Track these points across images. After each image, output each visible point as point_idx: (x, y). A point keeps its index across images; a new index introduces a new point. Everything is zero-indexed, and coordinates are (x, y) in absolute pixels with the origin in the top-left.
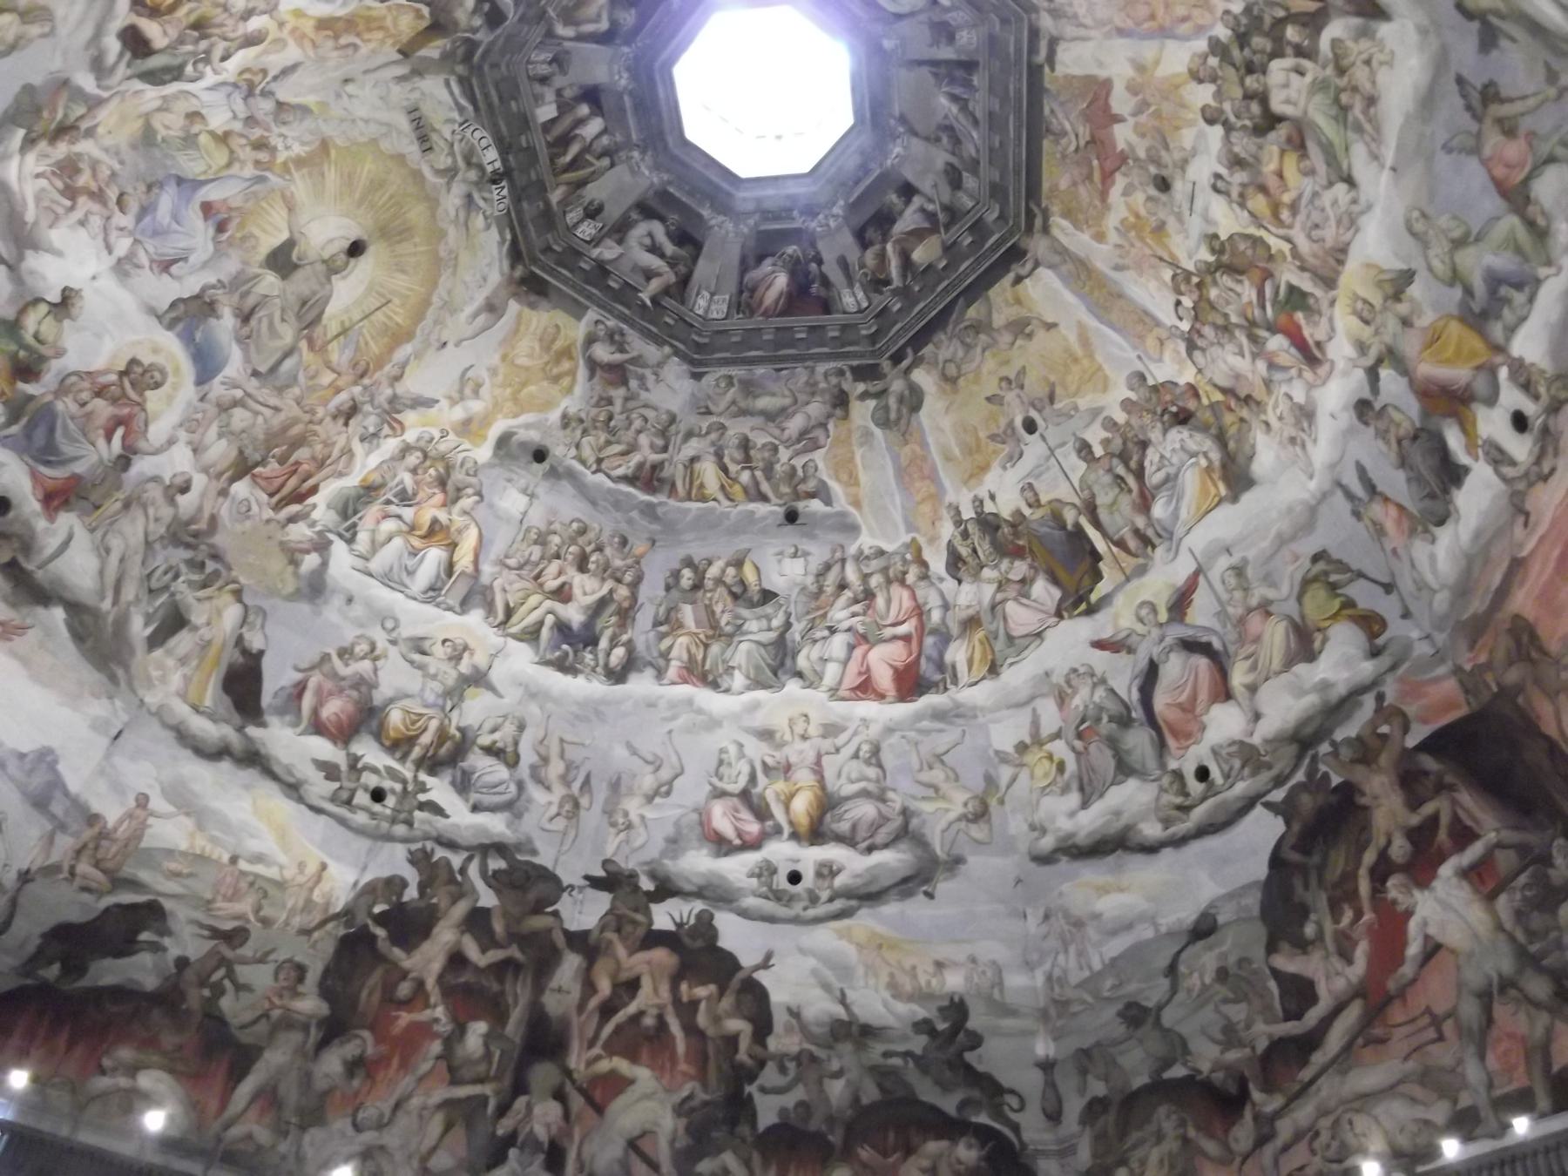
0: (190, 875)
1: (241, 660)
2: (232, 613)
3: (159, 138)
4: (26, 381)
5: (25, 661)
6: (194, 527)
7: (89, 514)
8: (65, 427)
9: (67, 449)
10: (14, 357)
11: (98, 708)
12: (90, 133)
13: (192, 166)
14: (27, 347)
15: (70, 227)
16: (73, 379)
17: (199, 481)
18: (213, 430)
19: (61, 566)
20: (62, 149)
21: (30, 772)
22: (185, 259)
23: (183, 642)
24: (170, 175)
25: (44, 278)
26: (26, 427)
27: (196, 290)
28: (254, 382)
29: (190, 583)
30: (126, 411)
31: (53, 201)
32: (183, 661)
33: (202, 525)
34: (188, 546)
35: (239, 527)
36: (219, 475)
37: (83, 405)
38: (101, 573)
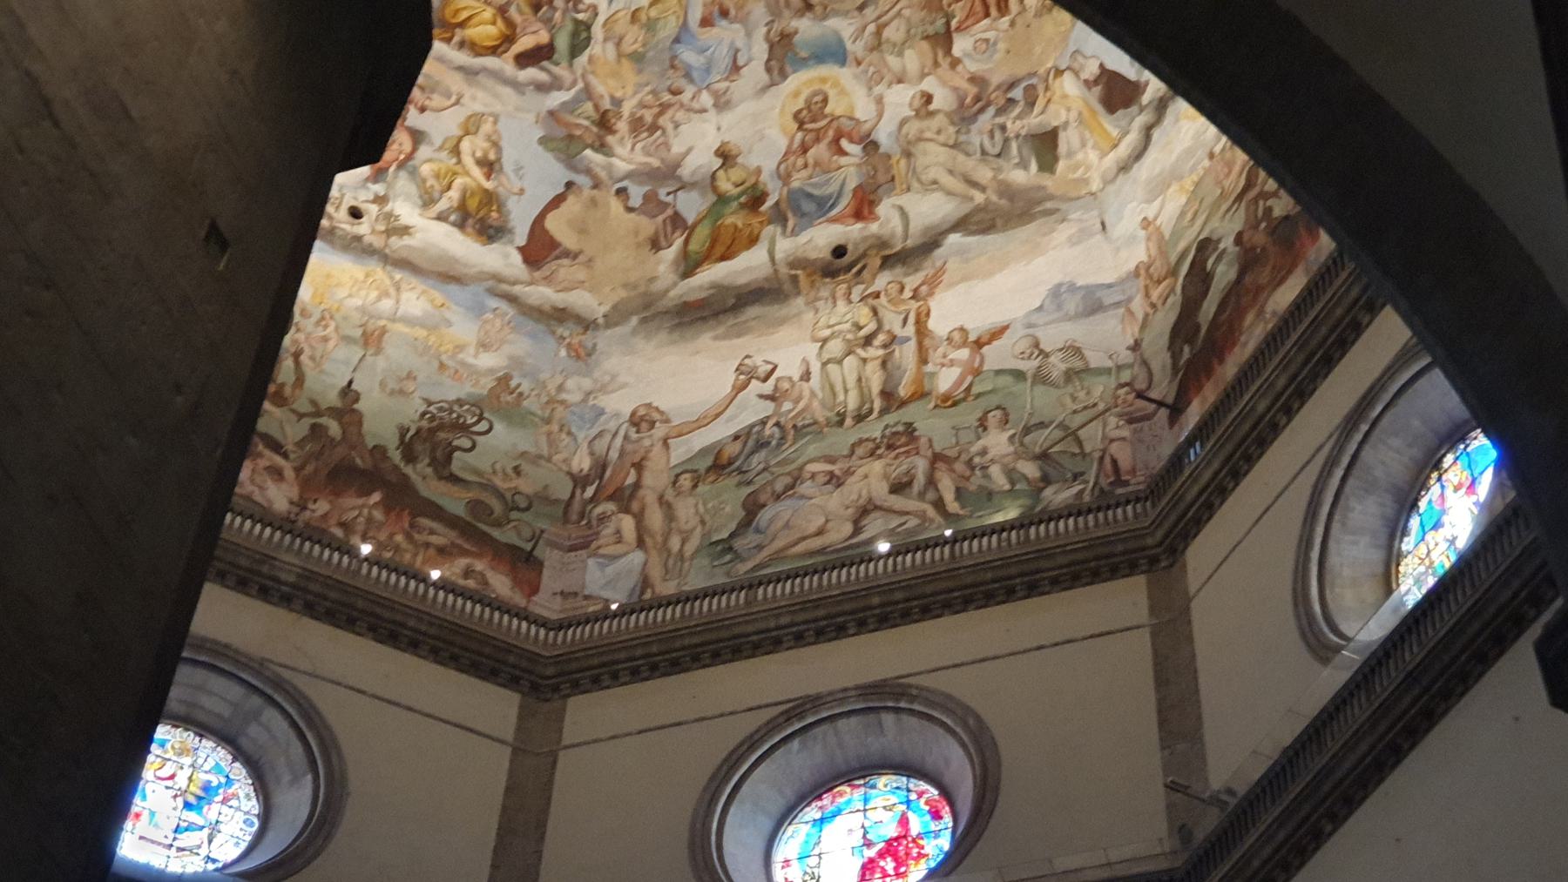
0: (1201, 202)
1: (1099, 88)
2: (1069, 85)
3: (641, 50)
4: (763, 203)
5: (965, 279)
6: (968, 100)
7: (894, 189)
8: (815, 185)
9: (833, 188)
10: (743, 206)
11: (1064, 232)
12: (617, 102)
13: (669, 28)
14: (739, 196)
15: (676, 136)
16: (783, 167)
17: (929, 85)
18: (893, 61)
19: (916, 225)
20: (622, 126)
21: (1059, 307)
22: (737, 51)
23: (1067, 140)
24: (671, 49)
25: (700, 167)
26: (795, 214)
27: (765, 46)
28: (870, 12)
29: (1019, 117)
30: (831, 133)
31: (652, 144)
32: (1084, 145)
33: (972, 90)
34: (982, 110)
35: (998, 56)
36: (936, 64)
37: (806, 166)
38: (949, 193)
